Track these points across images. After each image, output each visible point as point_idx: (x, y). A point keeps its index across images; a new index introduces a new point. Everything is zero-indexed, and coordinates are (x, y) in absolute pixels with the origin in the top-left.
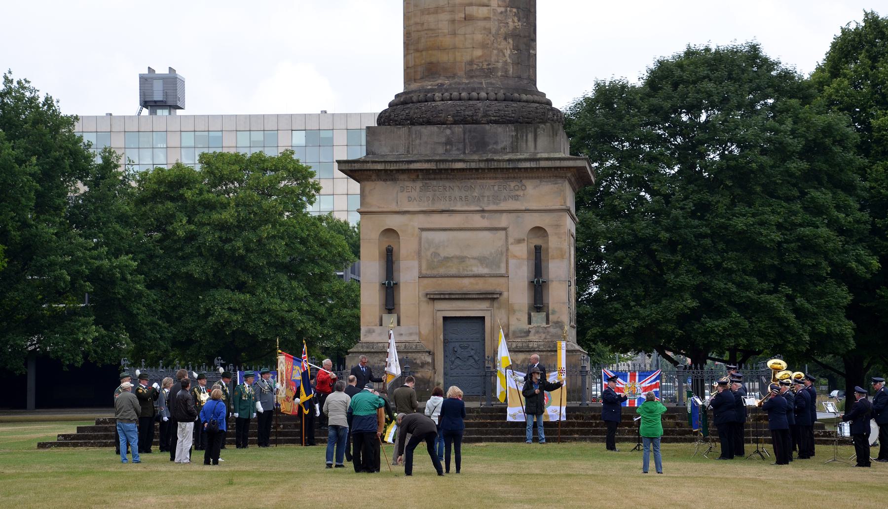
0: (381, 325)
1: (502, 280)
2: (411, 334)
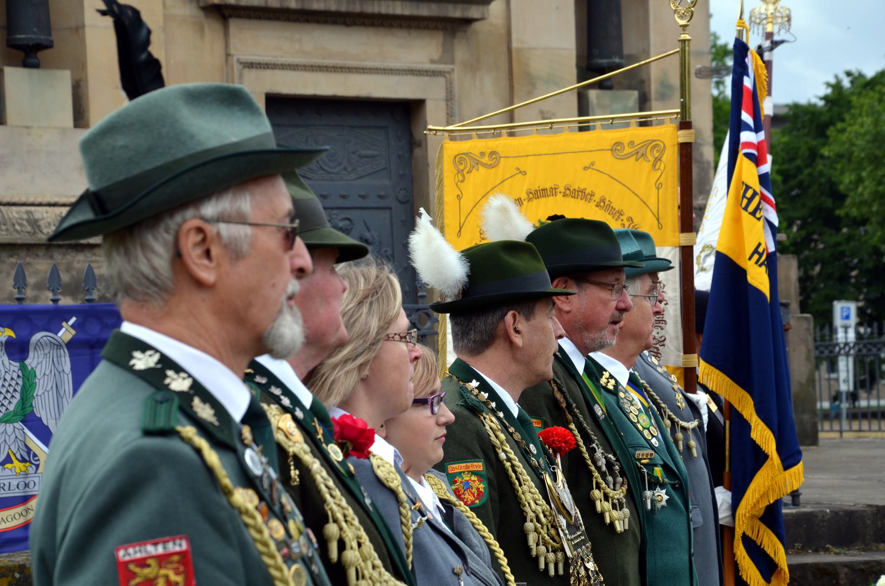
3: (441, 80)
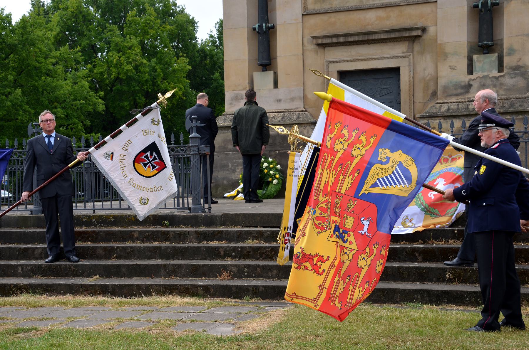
2: (292, 99)
3: (407, 59)
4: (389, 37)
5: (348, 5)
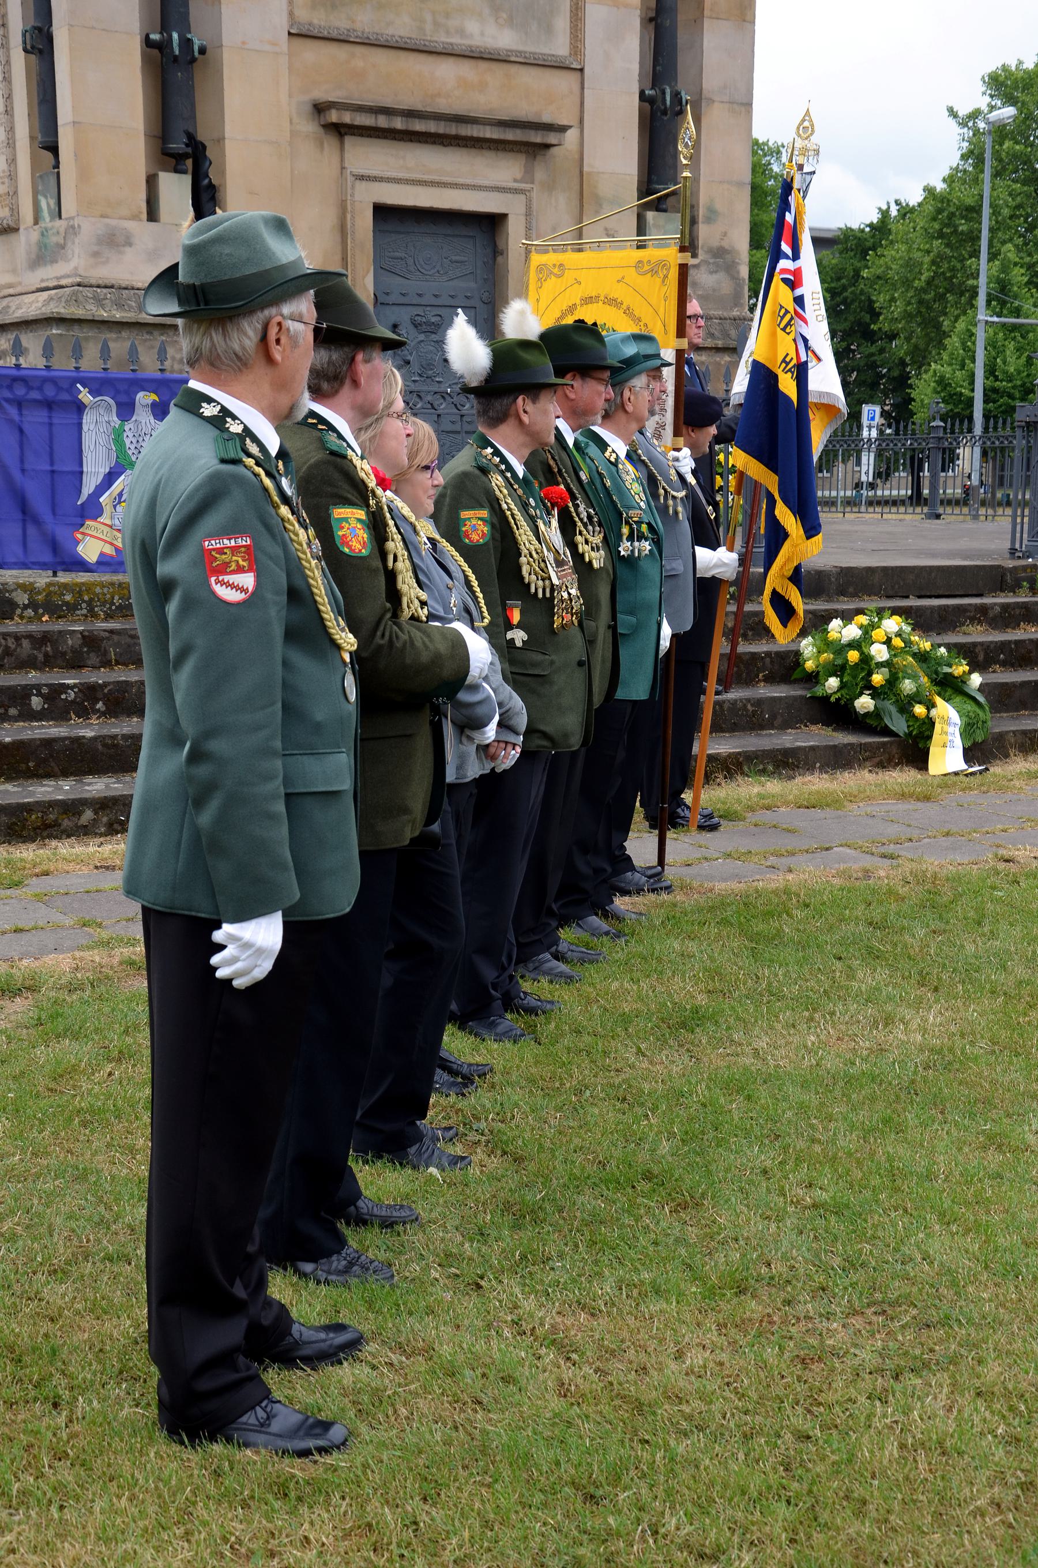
0: (152, 215)
1: (563, 83)
4: (502, 137)
5: (390, 31)
